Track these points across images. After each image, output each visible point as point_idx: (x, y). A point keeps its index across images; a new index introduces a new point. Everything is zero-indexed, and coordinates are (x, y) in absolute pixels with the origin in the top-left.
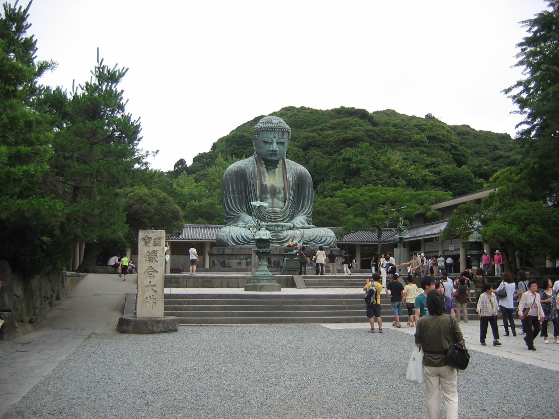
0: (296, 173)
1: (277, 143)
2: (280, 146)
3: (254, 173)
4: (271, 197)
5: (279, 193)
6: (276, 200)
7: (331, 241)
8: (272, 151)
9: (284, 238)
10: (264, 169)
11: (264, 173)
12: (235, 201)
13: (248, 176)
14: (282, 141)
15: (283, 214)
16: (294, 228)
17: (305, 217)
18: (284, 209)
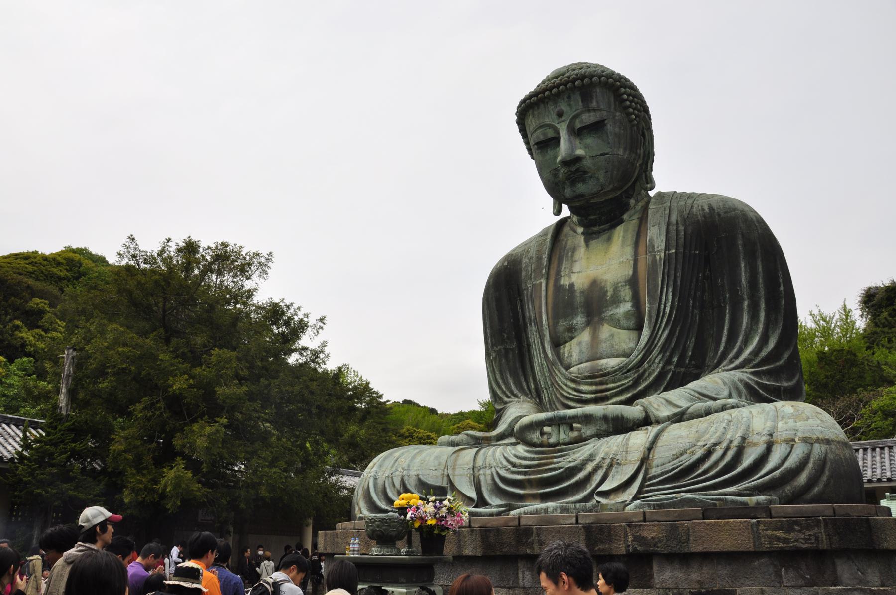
0: (688, 219)
1: (577, 133)
2: (589, 141)
3: (539, 259)
4: (588, 324)
5: (616, 301)
6: (606, 331)
7: (790, 463)
8: (565, 163)
9: (572, 471)
10: (576, 237)
11: (574, 250)
12: (500, 365)
13: (524, 273)
14: (588, 118)
15: (633, 375)
16: (646, 421)
17: (744, 375)
18: (636, 357)
